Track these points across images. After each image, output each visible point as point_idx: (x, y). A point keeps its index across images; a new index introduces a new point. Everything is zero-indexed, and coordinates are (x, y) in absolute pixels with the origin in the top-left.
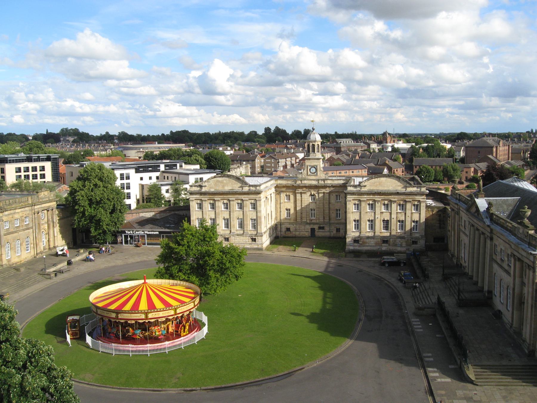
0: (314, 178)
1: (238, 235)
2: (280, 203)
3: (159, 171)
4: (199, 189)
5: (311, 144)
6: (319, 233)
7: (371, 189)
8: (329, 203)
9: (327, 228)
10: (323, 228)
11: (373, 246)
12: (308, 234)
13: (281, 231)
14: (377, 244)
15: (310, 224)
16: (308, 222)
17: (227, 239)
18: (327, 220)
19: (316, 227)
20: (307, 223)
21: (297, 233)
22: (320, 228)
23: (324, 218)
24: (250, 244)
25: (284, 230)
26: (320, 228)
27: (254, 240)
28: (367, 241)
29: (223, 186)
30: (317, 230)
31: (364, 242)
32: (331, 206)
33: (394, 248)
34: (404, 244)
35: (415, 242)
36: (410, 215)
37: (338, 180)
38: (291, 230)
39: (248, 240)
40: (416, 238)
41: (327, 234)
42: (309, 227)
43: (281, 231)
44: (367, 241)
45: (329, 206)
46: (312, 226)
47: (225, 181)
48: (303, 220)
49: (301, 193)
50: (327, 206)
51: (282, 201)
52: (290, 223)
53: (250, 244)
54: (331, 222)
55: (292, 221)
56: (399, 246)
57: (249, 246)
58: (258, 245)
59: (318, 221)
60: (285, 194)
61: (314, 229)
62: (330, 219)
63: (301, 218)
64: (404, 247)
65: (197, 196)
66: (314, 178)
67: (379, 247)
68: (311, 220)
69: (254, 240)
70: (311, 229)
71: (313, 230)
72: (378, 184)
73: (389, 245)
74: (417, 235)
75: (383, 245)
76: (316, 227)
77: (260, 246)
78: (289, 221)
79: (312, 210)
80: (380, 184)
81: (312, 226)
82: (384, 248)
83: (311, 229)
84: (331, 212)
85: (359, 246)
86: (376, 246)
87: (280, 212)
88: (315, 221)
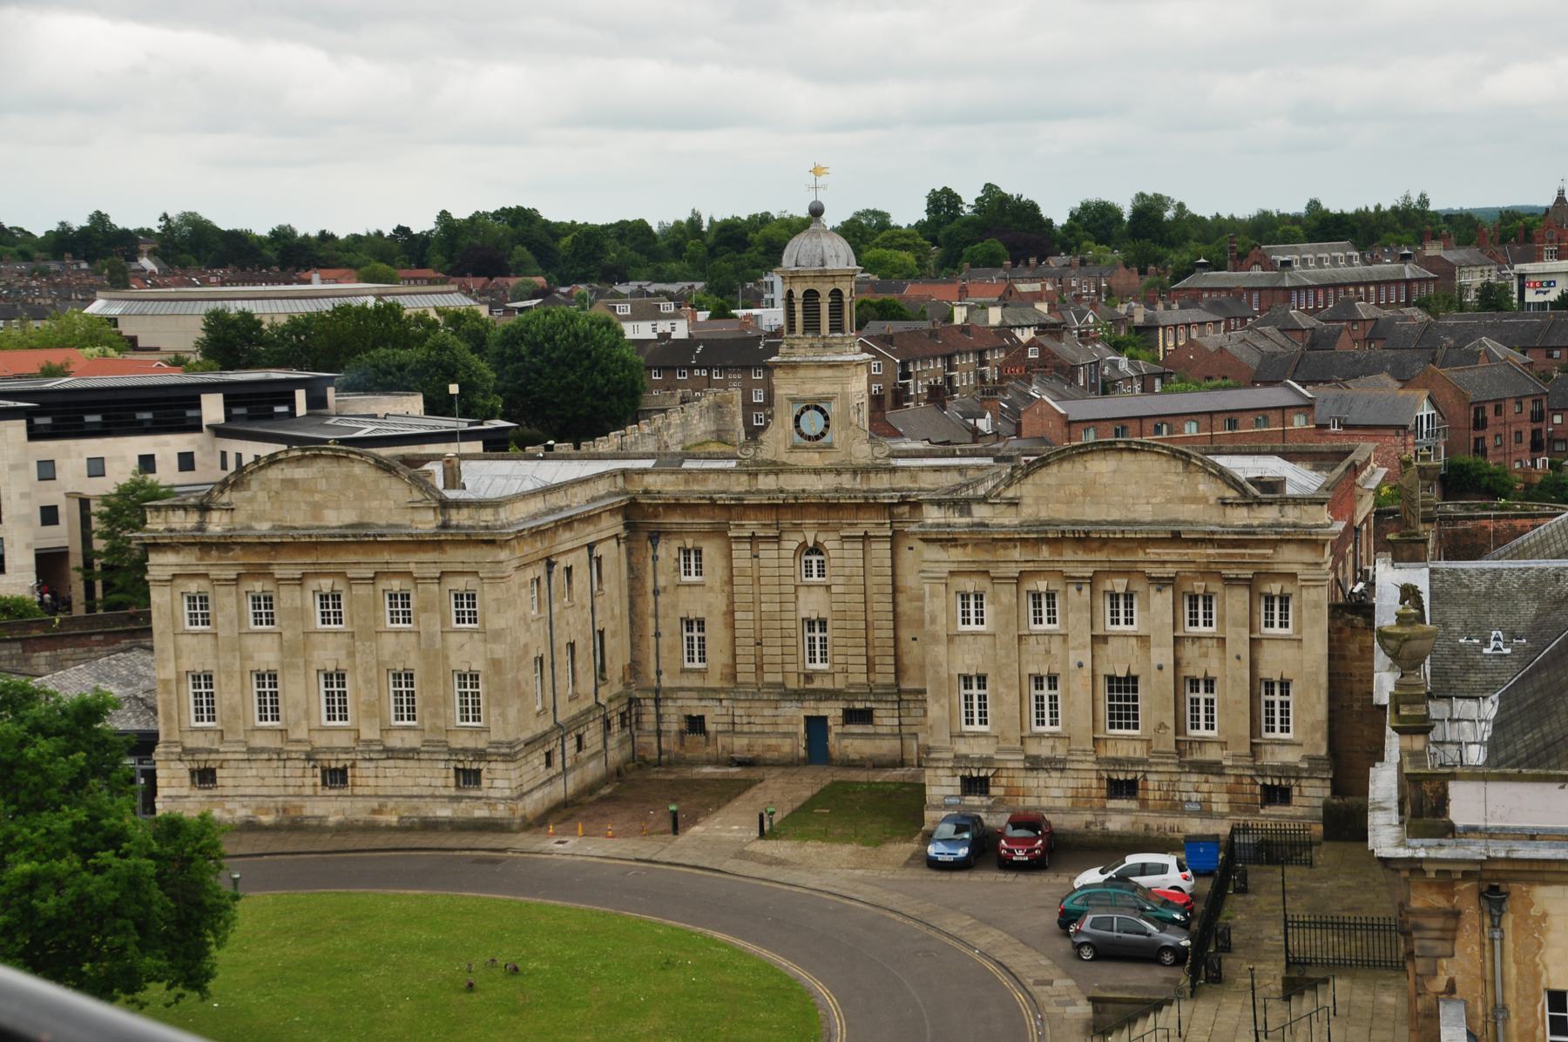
0: (814, 459)
1: (391, 753)
2: (656, 592)
3: (195, 427)
4: (192, 520)
5: (798, 293)
6: (848, 743)
7: (1044, 515)
8: (895, 590)
9: (886, 718)
10: (865, 716)
11: (1062, 811)
12: (797, 745)
13: (659, 733)
14: (1079, 800)
15: (800, 695)
16: (792, 683)
17: (336, 777)
18: (885, 675)
19: (832, 711)
20: (787, 694)
21: (740, 743)
22: (851, 716)
23: (870, 666)
24: (453, 799)
25: (673, 724)
26: (851, 716)
27: (468, 777)
28: (1032, 783)
29: (317, 508)
30: (835, 727)
31: (1012, 791)
32: (905, 606)
33: (1170, 821)
34: (1220, 803)
35: (1277, 795)
36: (1245, 652)
37: (938, 469)
38: (710, 727)
39: (436, 776)
40: (1285, 770)
41: (887, 747)
42: (794, 715)
43: (659, 733)
44: (1032, 783)
45: (895, 603)
46: (812, 708)
47: (322, 485)
48: (768, 678)
49: (753, 539)
50: (883, 605)
51: (662, 582)
52: (703, 693)
53: (453, 799)
54: (904, 686)
55: (714, 681)
56: (1193, 814)
57: (444, 812)
58: (490, 802)
59: (840, 683)
60: (676, 544)
61: (825, 718)
62: (898, 672)
63: (759, 667)
64: (1222, 816)
65: (188, 559)
66: (814, 459)
67: (1089, 817)
68: (809, 677)
69: (468, 777)
70: (809, 720)
71: (816, 726)
72: (1077, 489)
73: (1144, 804)
74: (1290, 756)
75: (1112, 804)
76: (832, 711)
77: (501, 812)
78: (696, 682)
79: (811, 624)
80: (1089, 490)
81: (812, 708)
82: (1116, 824)
83: (809, 720)
84: (905, 634)
85: (989, 810)
86: (1074, 809)
87: (657, 635)
88: (827, 684)
